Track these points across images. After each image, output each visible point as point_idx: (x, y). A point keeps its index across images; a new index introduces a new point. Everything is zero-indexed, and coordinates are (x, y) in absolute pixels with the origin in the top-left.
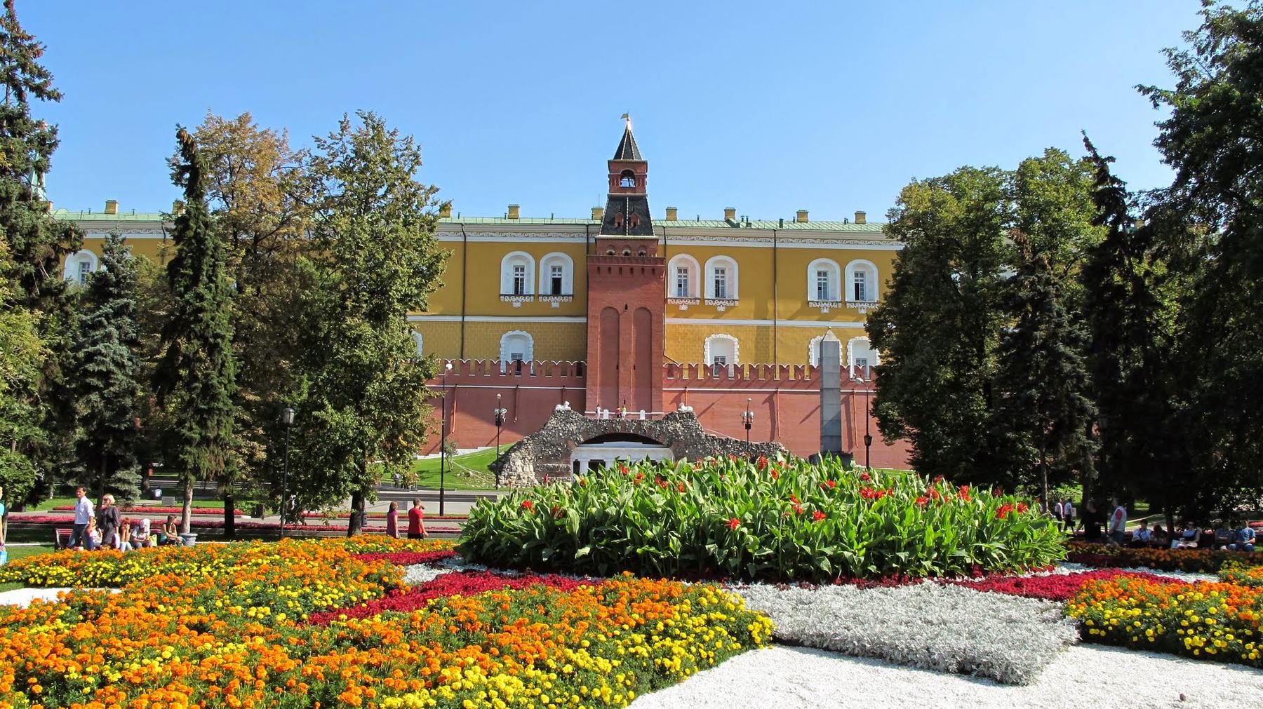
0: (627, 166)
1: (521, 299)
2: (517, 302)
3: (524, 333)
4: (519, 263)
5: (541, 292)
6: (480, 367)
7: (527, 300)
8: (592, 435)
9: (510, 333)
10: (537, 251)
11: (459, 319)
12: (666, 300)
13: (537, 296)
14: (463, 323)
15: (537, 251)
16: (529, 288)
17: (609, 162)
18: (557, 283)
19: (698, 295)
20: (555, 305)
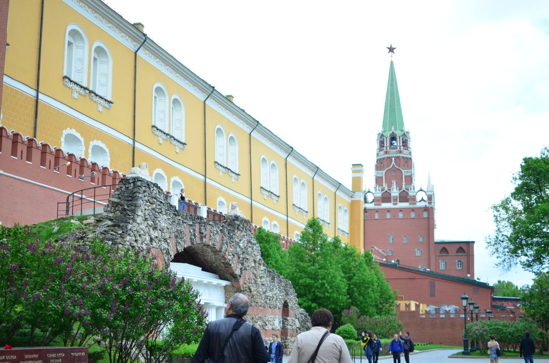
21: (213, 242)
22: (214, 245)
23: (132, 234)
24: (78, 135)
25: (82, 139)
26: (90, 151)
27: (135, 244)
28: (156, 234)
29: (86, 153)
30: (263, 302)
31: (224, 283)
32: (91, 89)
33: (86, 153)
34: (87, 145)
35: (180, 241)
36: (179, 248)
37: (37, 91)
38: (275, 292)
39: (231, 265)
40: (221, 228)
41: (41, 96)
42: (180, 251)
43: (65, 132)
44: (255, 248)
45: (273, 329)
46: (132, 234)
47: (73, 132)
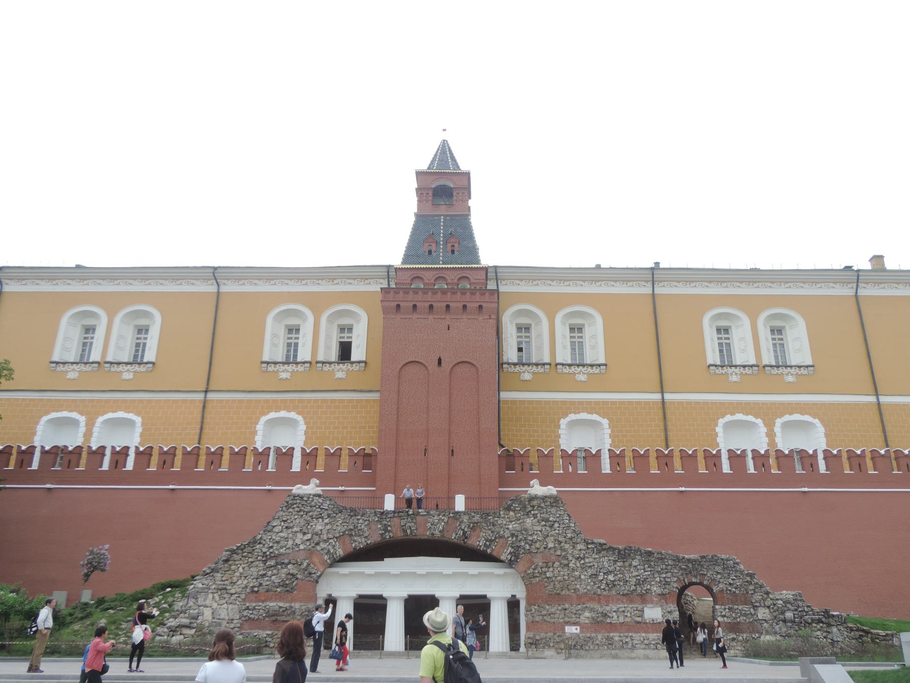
0: (444, 190)
1: (290, 368)
2: (285, 373)
3: (293, 415)
4: (293, 321)
5: (321, 358)
7: (300, 368)
8: (360, 542)
9: (273, 415)
10: (317, 303)
11: (201, 396)
12: (501, 365)
15: (317, 303)
16: (304, 354)
17: (419, 174)
22: (433, 534)
25: (759, 421)
26: (777, 429)
27: (264, 550)
28: (306, 537)
29: (771, 435)
30: (589, 588)
32: (766, 361)
33: (771, 435)
34: (770, 425)
37: (662, 392)
38: (635, 574)
41: (668, 397)
43: (721, 422)
44: (556, 525)
45: (638, 623)
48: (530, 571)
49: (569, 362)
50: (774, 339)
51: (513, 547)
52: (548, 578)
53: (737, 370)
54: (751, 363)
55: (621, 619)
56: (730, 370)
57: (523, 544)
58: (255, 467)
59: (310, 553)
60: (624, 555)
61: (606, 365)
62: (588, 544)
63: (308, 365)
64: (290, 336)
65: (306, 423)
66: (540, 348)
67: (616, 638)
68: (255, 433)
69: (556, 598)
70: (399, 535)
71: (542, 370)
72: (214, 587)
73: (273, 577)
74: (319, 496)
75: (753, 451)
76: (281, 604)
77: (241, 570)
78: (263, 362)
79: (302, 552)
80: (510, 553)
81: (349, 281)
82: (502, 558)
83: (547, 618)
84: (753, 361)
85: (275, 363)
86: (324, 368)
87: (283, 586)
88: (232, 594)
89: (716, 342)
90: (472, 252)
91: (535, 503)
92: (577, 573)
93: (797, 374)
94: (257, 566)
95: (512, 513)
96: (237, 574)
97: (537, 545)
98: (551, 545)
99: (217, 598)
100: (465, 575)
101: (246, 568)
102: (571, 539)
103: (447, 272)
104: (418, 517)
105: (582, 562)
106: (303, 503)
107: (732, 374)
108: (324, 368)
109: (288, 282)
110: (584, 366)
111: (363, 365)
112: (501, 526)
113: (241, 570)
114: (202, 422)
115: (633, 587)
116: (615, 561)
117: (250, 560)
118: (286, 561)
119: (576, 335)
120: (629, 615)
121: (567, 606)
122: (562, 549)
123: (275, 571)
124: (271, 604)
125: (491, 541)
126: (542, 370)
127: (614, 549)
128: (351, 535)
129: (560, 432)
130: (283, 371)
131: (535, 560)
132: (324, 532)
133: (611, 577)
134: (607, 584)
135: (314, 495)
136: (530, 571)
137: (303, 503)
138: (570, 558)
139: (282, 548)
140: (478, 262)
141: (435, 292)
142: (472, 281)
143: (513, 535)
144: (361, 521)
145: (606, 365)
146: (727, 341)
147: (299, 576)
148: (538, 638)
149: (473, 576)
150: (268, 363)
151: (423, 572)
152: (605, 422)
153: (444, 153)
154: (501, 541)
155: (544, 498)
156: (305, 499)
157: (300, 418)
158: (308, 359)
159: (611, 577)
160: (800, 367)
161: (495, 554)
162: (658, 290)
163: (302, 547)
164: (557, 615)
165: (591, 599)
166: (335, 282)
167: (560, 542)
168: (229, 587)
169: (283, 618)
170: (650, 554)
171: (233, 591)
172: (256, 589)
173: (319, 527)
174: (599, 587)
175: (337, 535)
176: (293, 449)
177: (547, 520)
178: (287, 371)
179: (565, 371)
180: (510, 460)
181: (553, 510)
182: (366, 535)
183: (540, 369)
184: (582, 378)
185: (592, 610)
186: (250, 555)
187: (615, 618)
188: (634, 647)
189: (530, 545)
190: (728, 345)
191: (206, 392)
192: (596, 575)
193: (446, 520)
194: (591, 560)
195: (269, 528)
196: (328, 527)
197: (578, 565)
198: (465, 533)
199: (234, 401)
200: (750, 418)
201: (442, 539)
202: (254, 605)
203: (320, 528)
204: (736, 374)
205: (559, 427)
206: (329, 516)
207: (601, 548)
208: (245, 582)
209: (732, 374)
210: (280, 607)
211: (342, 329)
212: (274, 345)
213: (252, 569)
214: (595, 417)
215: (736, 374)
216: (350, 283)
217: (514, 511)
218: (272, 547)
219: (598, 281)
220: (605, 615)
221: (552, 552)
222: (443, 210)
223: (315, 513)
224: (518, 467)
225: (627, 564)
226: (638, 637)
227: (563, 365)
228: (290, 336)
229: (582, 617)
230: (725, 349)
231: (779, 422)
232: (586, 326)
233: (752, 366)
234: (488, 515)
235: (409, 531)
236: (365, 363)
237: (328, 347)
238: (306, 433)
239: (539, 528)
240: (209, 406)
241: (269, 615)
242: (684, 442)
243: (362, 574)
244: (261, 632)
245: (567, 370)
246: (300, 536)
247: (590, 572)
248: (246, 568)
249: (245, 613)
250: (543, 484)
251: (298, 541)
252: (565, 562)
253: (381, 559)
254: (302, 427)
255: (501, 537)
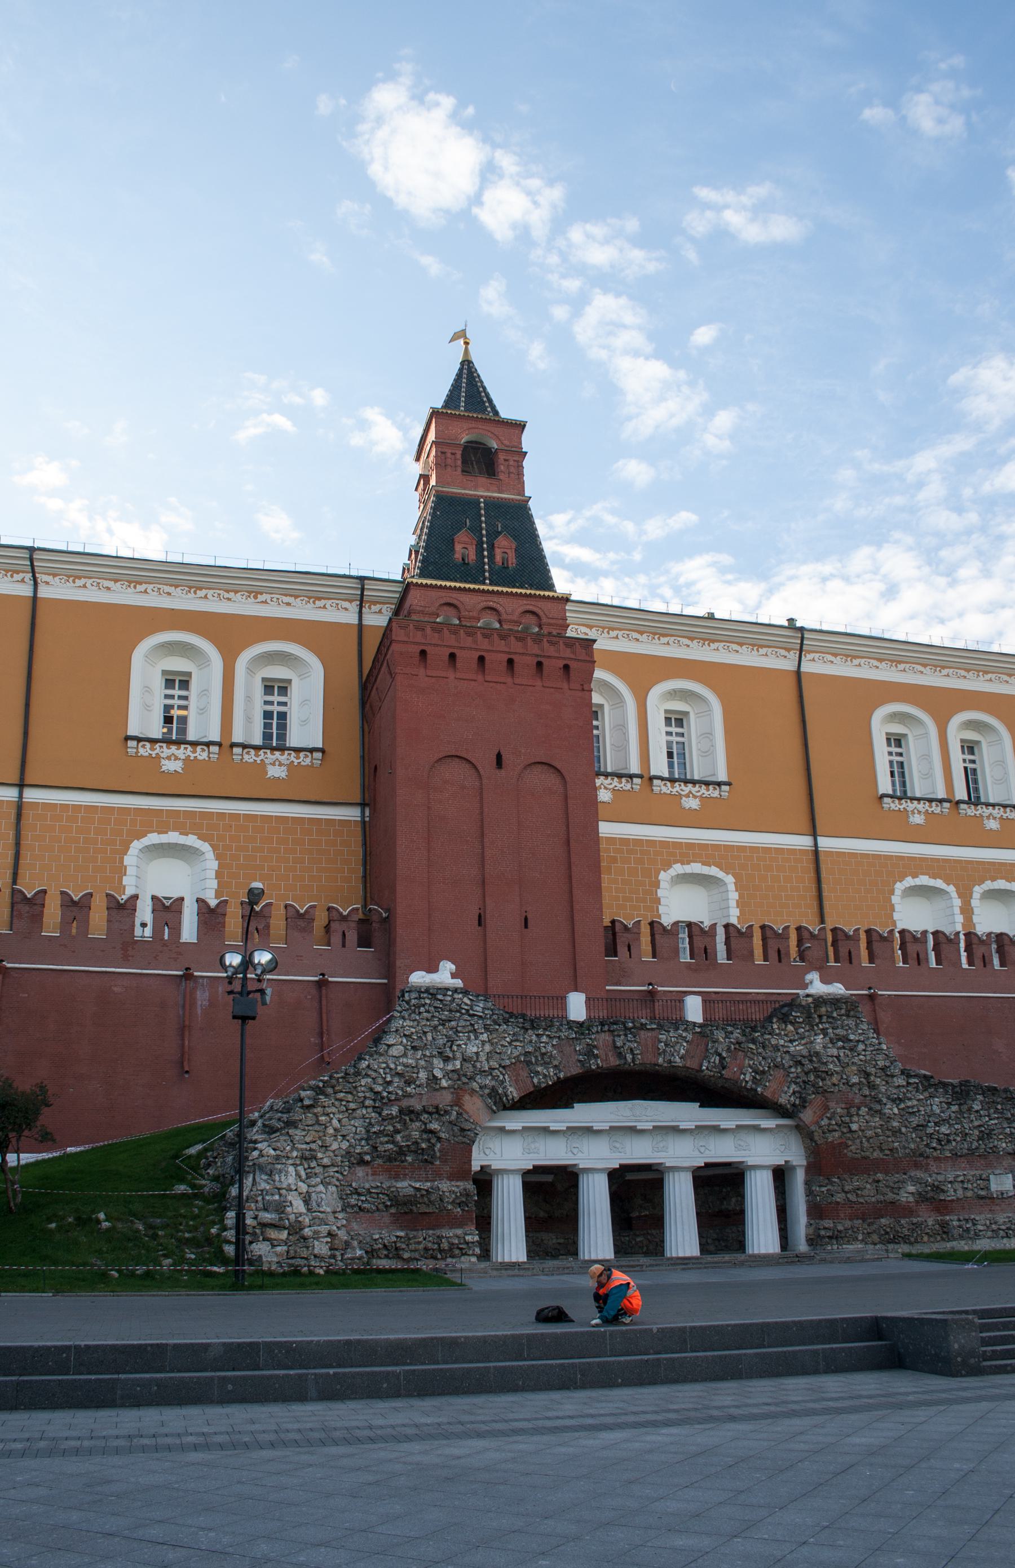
1: (182, 752)
2: (173, 761)
3: (191, 840)
4: (178, 664)
5: (238, 737)
6: (76, 908)
7: (201, 754)
8: (546, 1075)
9: (153, 838)
10: (230, 635)
13: (227, 745)
14: (20, 806)
15: (230, 635)
18: (276, 723)
19: (635, 768)
20: (276, 772)
21: (668, 1057)
22: (670, 1061)
23: (374, 1074)
24: (939, 883)
25: (951, 889)
27: (379, 1088)
28: (450, 1067)
29: (967, 911)
30: (912, 1146)
31: (770, 1123)
33: (967, 911)
34: (965, 896)
35: (539, 1069)
36: (535, 1080)
37: (814, 835)
38: (976, 1123)
39: (756, 1090)
40: (698, 1030)
41: (824, 843)
42: (543, 1085)
43: (899, 887)
44: (861, 1047)
45: (982, 1198)
46: (374, 1074)
47: (924, 880)
48: (825, 1122)
49: (666, 775)
50: (964, 761)
51: (796, 1083)
52: (851, 1131)
53: (921, 806)
54: (940, 797)
55: (960, 1193)
56: (911, 806)
57: (812, 1078)
58: (157, 931)
59: (458, 1092)
60: (961, 1093)
61: (729, 784)
62: (909, 1076)
63: (214, 749)
64: (170, 692)
65: (218, 857)
66: (622, 748)
67: (955, 1223)
68: (122, 871)
69: (861, 1166)
70: (614, 1061)
71: (629, 786)
72: (295, 1154)
73: (398, 1137)
74: (465, 992)
75: (936, 934)
76: (417, 1185)
77: (335, 1122)
78: (127, 738)
79: (444, 1092)
80: (794, 1093)
81: (287, 599)
82: (783, 1100)
83: (852, 1197)
84: (941, 794)
85: (153, 741)
86: (246, 757)
87: (416, 1152)
88: (324, 1167)
89: (888, 758)
90: (532, 567)
91: (823, 1010)
92: (895, 1124)
93: (1001, 818)
94: (363, 1117)
95: (790, 1027)
96: (331, 1131)
97: (835, 1079)
98: (855, 1079)
99: (303, 1174)
100: (716, 1130)
101: (345, 1121)
102: (883, 1069)
103: (501, 600)
104: (642, 1032)
105: (902, 1106)
106: (438, 1004)
107: (913, 812)
108: (246, 757)
109: (171, 589)
110: (694, 782)
111: (319, 755)
112: (776, 1048)
113: (335, 1122)
114: (18, 844)
115: (975, 1145)
116: (949, 1104)
117: (352, 1106)
118: (418, 1107)
119: (674, 729)
120: (970, 1186)
121: (880, 1176)
122: (872, 1086)
123: (398, 1126)
124: (399, 1185)
125: (763, 1072)
126: (629, 786)
127: (945, 1085)
128: (528, 1063)
129: (660, 893)
130: (169, 758)
131: (832, 1104)
132: (483, 1057)
133: (944, 1129)
134: (939, 1141)
135: (456, 990)
136: (825, 1122)
137: (438, 1004)
138: (885, 1100)
139: (408, 1083)
140: (551, 587)
141: (471, 631)
142: (544, 620)
143: (799, 1063)
144: (544, 1039)
145: (729, 784)
146: (899, 759)
147: (443, 1135)
148: (840, 1227)
149: (765, 1130)
150: (139, 740)
151: (649, 1126)
152: (730, 880)
153: (468, 392)
154: (779, 1073)
155: (835, 1002)
156: (440, 997)
157: (205, 847)
158: (217, 738)
159: (944, 1129)
160: (1005, 806)
161: (768, 1094)
162: (807, 667)
163: (444, 1083)
164: (866, 1192)
165: (917, 1166)
166: (261, 598)
167: (868, 1075)
168: (320, 1155)
169: (424, 1209)
170: (994, 1090)
171: (326, 1161)
172: (368, 1158)
173: (472, 1049)
174: (927, 1146)
175: (508, 1062)
176: (182, 899)
177: (846, 1039)
178: (177, 758)
179: (664, 790)
180: (614, 937)
181: (851, 1022)
182: (556, 1063)
183: (625, 785)
184: (693, 804)
185: (917, 1181)
186: (350, 1097)
187: (952, 1193)
188: (977, 1235)
189: (823, 1080)
190: (901, 765)
191: (21, 786)
192: (925, 1126)
193: (689, 1037)
194: (915, 1103)
195: (382, 1048)
196: (488, 1048)
197: (896, 1111)
198: (722, 1058)
199: (77, 808)
200: (939, 883)
201: (684, 1067)
202: (367, 1186)
203: (475, 1049)
204: (919, 812)
205: (657, 884)
206: (486, 1028)
207: (928, 1083)
208: (345, 1145)
209: (913, 812)
210: (418, 1189)
211: (268, 689)
212: (147, 707)
213: (352, 1122)
214: (714, 871)
215: (919, 812)
216: (288, 604)
217: (792, 1023)
218: (389, 1083)
219: (714, 641)
220: (937, 1188)
221: (855, 1089)
222: (482, 491)
223: (462, 1023)
224: (622, 950)
225: (965, 1108)
226: (982, 1218)
227: (662, 779)
228: (170, 692)
229: (902, 1191)
230: (899, 771)
231: (978, 890)
232: (692, 716)
233: (941, 801)
234: (754, 1029)
235: (629, 1057)
236: (322, 751)
237: (249, 719)
238: (218, 875)
239: (835, 1052)
240: (28, 814)
241: (396, 1200)
242: (846, 916)
243: (546, 1131)
244: (385, 1232)
245: (666, 788)
246: (438, 1062)
247: (915, 1121)
248: (345, 1121)
249: (353, 1202)
250: (825, 981)
251: (439, 1074)
252: (878, 1107)
253: (568, 1105)
254: (212, 864)
255: (776, 1066)
